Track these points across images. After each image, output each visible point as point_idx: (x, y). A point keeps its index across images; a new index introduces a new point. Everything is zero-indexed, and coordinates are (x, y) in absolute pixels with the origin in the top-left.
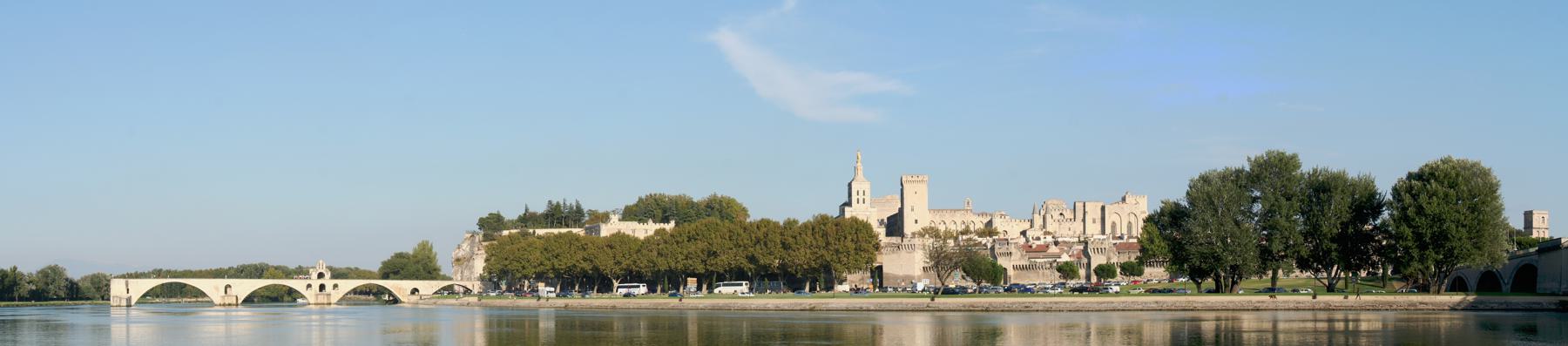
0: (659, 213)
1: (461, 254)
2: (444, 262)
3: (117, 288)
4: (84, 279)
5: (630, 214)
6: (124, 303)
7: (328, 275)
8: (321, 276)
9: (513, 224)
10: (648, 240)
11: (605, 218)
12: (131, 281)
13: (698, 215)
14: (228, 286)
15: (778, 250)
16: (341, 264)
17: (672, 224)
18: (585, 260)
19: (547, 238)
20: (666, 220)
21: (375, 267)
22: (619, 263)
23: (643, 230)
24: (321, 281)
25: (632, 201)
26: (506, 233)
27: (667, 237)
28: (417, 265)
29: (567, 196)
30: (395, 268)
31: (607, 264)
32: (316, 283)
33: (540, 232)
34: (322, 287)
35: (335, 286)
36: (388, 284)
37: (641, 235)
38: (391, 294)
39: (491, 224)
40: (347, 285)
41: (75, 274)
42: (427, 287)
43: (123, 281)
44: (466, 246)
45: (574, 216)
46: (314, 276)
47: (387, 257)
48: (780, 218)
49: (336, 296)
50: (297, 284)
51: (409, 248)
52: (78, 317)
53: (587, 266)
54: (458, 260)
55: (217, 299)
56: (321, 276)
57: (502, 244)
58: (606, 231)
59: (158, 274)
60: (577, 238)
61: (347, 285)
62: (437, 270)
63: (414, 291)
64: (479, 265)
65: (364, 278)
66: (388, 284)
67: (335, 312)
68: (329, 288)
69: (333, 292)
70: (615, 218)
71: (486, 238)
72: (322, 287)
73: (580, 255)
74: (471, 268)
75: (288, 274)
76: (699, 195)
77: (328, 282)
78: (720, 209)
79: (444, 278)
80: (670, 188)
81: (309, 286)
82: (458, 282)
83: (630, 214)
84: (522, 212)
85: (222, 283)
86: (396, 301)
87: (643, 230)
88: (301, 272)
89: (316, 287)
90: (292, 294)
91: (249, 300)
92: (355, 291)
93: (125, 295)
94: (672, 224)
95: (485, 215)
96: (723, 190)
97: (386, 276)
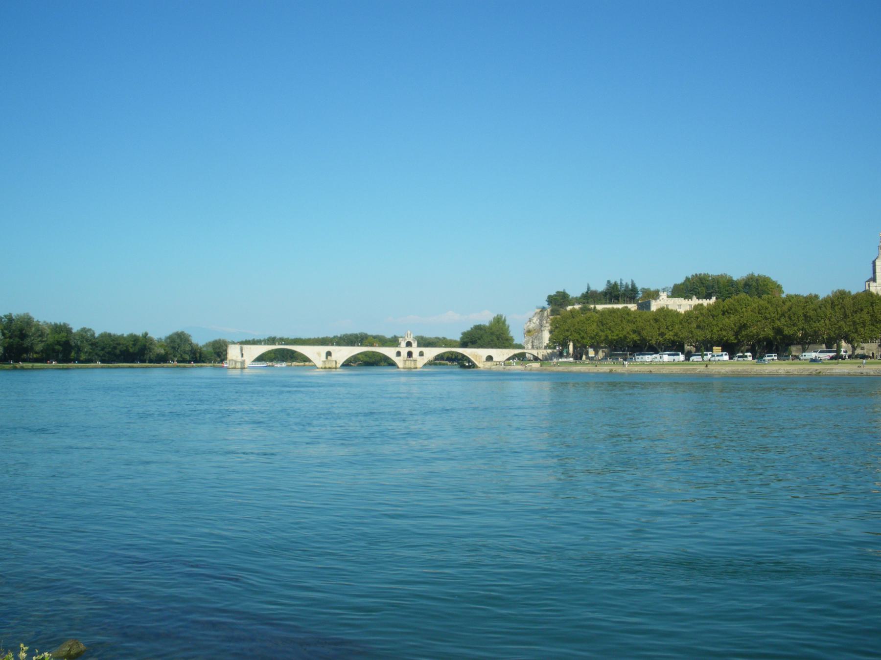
0: (703, 290)
1: (532, 326)
2: (517, 334)
3: (233, 352)
4: (207, 345)
5: (678, 291)
7: (415, 344)
8: (409, 344)
9: (577, 301)
10: (688, 314)
11: (655, 295)
12: (245, 346)
13: (737, 292)
14: (329, 354)
15: (801, 324)
16: (430, 334)
18: (634, 332)
19: (603, 313)
20: (708, 297)
21: (457, 337)
22: (662, 334)
23: (683, 305)
24: (409, 349)
25: (680, 280)
26: (569, 308)
27: (704, 311)
28: (492, 335)
29: (624, 277)
30: (475, 337)
31: (652, 335)
32: (404, 351)
33: (600, 307)
34: (410, 354)
35: (421, 354)
36: (467, 352)
37: (682, 311)
38: (469, 361)
39: (559, 301)
40: (431, 353)
41: (200, 340)
42: (500, 355)
43: (238, 347)
44: (536, 320)
45: (630, 294)
46: (403, 344)
47: (468, 328)
49: (421, 362)
50: (389, 352)
51: (485, 318)
53: (636, 337)
54: (529, 331)
55: (319, 364)
56: (409, 344)
57: (564, 319)
58: (654, 306)
59: (272, 341)
60: (626, 311)
61: (431, 353)
62: (511, 339)
63: (490, 358)
64: (546, 336)
65: (446, 346)
66: (467, 352)
67: (421, 374)
68: (416, 355)
69: (419, 358)
70: (663, 296)
71: (553, 312)
72: (410, 354)
73: (629, 328)
74: (540, 339)
76: (738, 274)
77: (416, 350)
78: (757, 286)
79: (520, 346)
80: (713, 268)
81: (399, 354)
82: (530, 352)
83: (678, 291)
84: (585, 290)
85: (324, 349)
86: (474, 366)
87: (683, 305)
88: (394, 342)
90: (389, 362)
91: (347, 364)
92: (439, 357)
94: (714, 299)
95: (553, 293)
96: (760, 270)
97: (464, 345)
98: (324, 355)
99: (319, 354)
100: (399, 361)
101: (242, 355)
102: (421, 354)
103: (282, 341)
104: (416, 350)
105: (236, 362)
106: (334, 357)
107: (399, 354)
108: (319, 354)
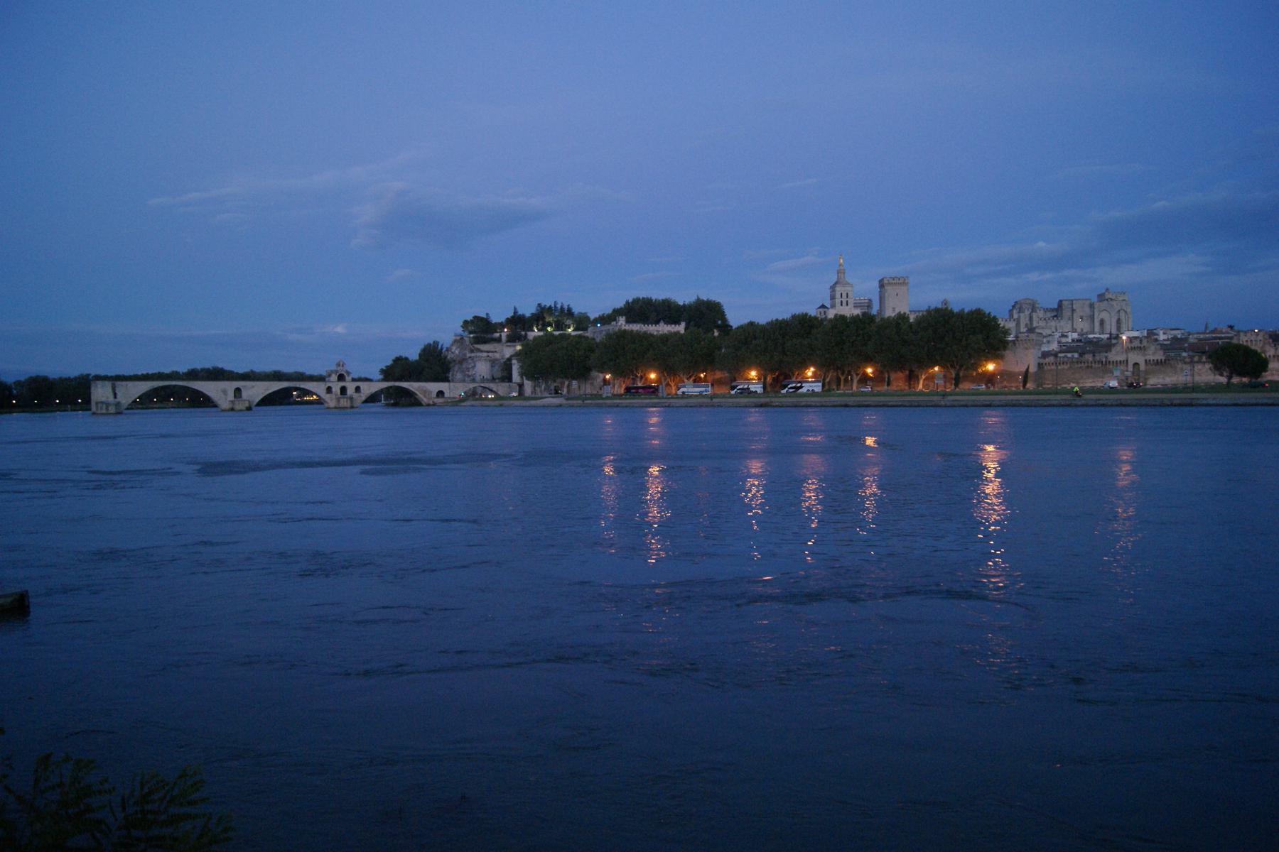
3: (101, 392)
6: (112, 410)
17: (683, 324)
34: (343, 390)
35: (358, 389)
43: (108, 384)
46: (334, 377)
48: (786, 315)
52: (65, 423)
55: (225, 405)
69: (355, 395)
72: (343, 390)
75: (311, 378)
81: (329, 390)
85: (231, 386)
89: (336, 388)
93: (111, 399)
98: (231, 396)
99: (225, 392)
100: (331, 401)
101: (115, 396)
102: (358, 389)
103: (160, 376)
104: (351, 387)
105: (108, 405)
106: (245, 394)
107: (329, 390)
108: (225, 392)
